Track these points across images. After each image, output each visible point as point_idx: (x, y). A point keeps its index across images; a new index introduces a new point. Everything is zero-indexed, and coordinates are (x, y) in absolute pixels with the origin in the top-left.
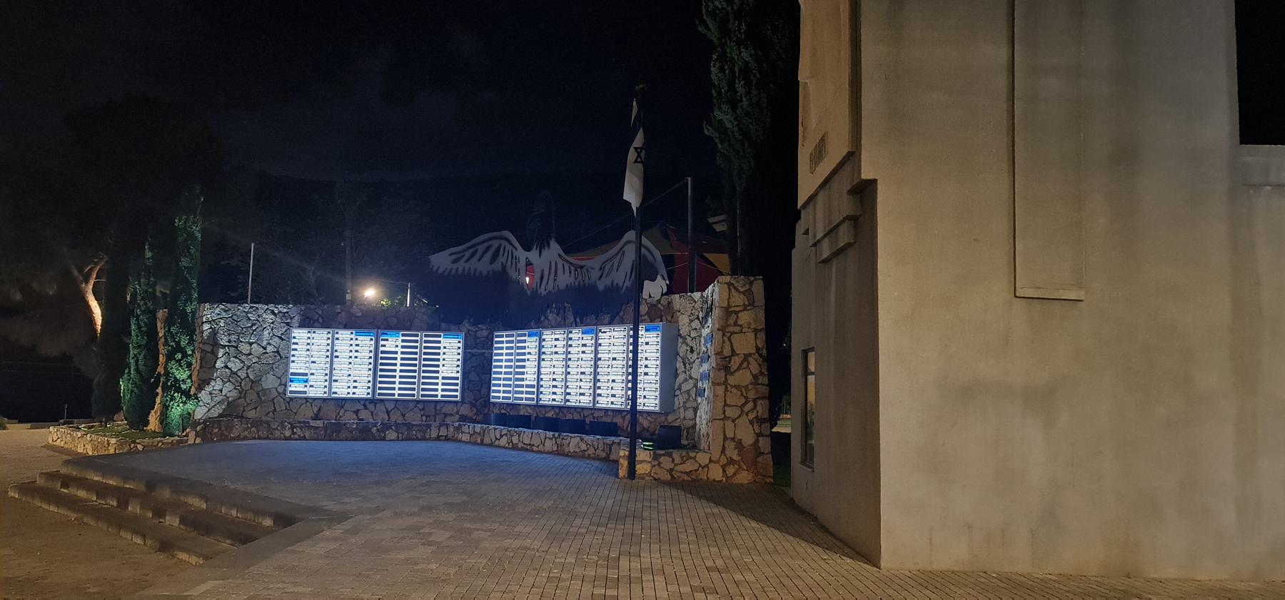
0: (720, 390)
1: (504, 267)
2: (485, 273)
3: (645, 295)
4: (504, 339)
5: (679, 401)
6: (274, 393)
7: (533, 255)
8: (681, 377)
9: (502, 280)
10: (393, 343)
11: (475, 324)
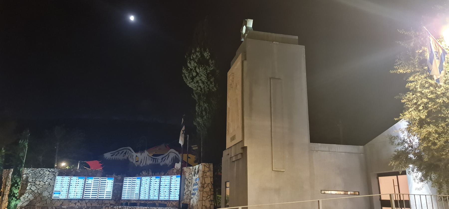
0: (202, 192)
1: (128, 158)
2: (121, 159)
3: (175, 167)
4: (128, 180)
5: (185, 197)
6: (47, 198)
7: (138, 155)
8: (186, 190)
9: (127, 161)
10: (91, 181)
11: (117, 175)
